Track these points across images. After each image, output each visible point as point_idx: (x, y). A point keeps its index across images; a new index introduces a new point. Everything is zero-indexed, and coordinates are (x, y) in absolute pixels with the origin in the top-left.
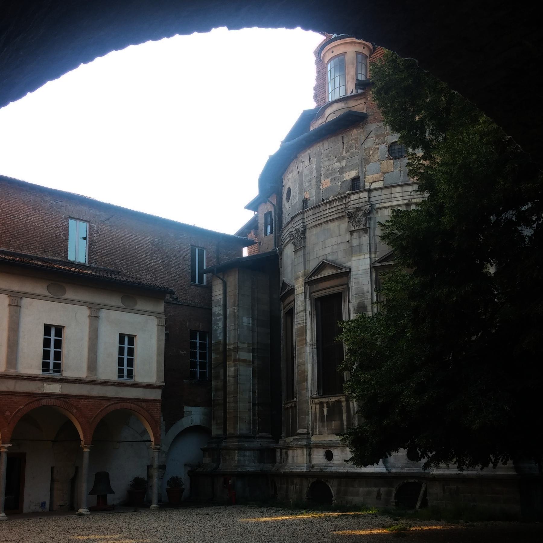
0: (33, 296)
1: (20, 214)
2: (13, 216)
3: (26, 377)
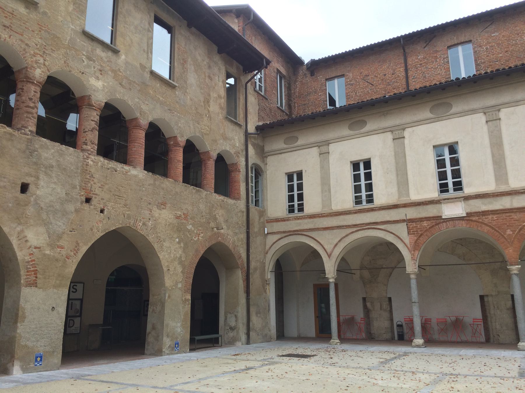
0: (513, 104)
1: (522, 35)
2: (515, 40)
3: (523, 191)
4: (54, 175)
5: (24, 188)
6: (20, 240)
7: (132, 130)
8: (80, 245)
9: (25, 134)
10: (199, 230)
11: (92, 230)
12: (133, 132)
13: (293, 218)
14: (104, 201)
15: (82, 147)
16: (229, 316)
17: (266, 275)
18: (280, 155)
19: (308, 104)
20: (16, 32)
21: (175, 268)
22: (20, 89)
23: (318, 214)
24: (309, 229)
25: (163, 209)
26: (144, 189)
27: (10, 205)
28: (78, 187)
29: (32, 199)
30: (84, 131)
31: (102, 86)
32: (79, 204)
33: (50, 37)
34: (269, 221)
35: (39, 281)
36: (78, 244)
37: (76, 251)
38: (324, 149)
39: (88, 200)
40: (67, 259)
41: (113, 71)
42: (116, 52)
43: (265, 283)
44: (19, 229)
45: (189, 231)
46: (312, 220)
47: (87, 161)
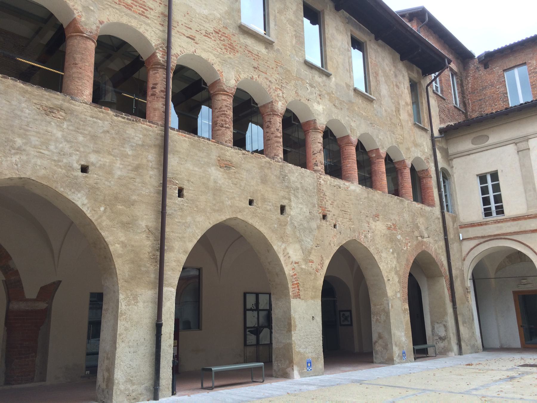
4: (300, 196)
5: (283, 209)
6: (285, 256)
7: (345, 147)
8: (324, 258)
9: (278, 162)
10: (406, 239)
11: (330, 244)
12: (345, 149)
13: (493, 222)
14: (335, 217)
15: (313, 169)
16: (436, 326)
17: (466, 283)
18: (468, 157)
19: (485, 98)
20: (262, 71)
21: (393, 278)
22: (268, 122)
23: (523, 216)
24: (514, 233)
25: (377, 220)
26: (361, 203)
27: (276, 226)
28: (316, 205)
29: (289, 219)
30: (314, 153)
31: (322, 110)
32: (319, 221)
33: (284, 71)
34: (463, 226)
35: (301, 293)
36: (322, 258)
37: (322, 264)
38: (522, 146)
39: (324, 217)
40: (317, 273)
41: (328, 94)
42: (328, 75)
43: (467, 290)
44: (283, 247)
45: (399, 241)
46: (515, 222)
47: (320, 181)
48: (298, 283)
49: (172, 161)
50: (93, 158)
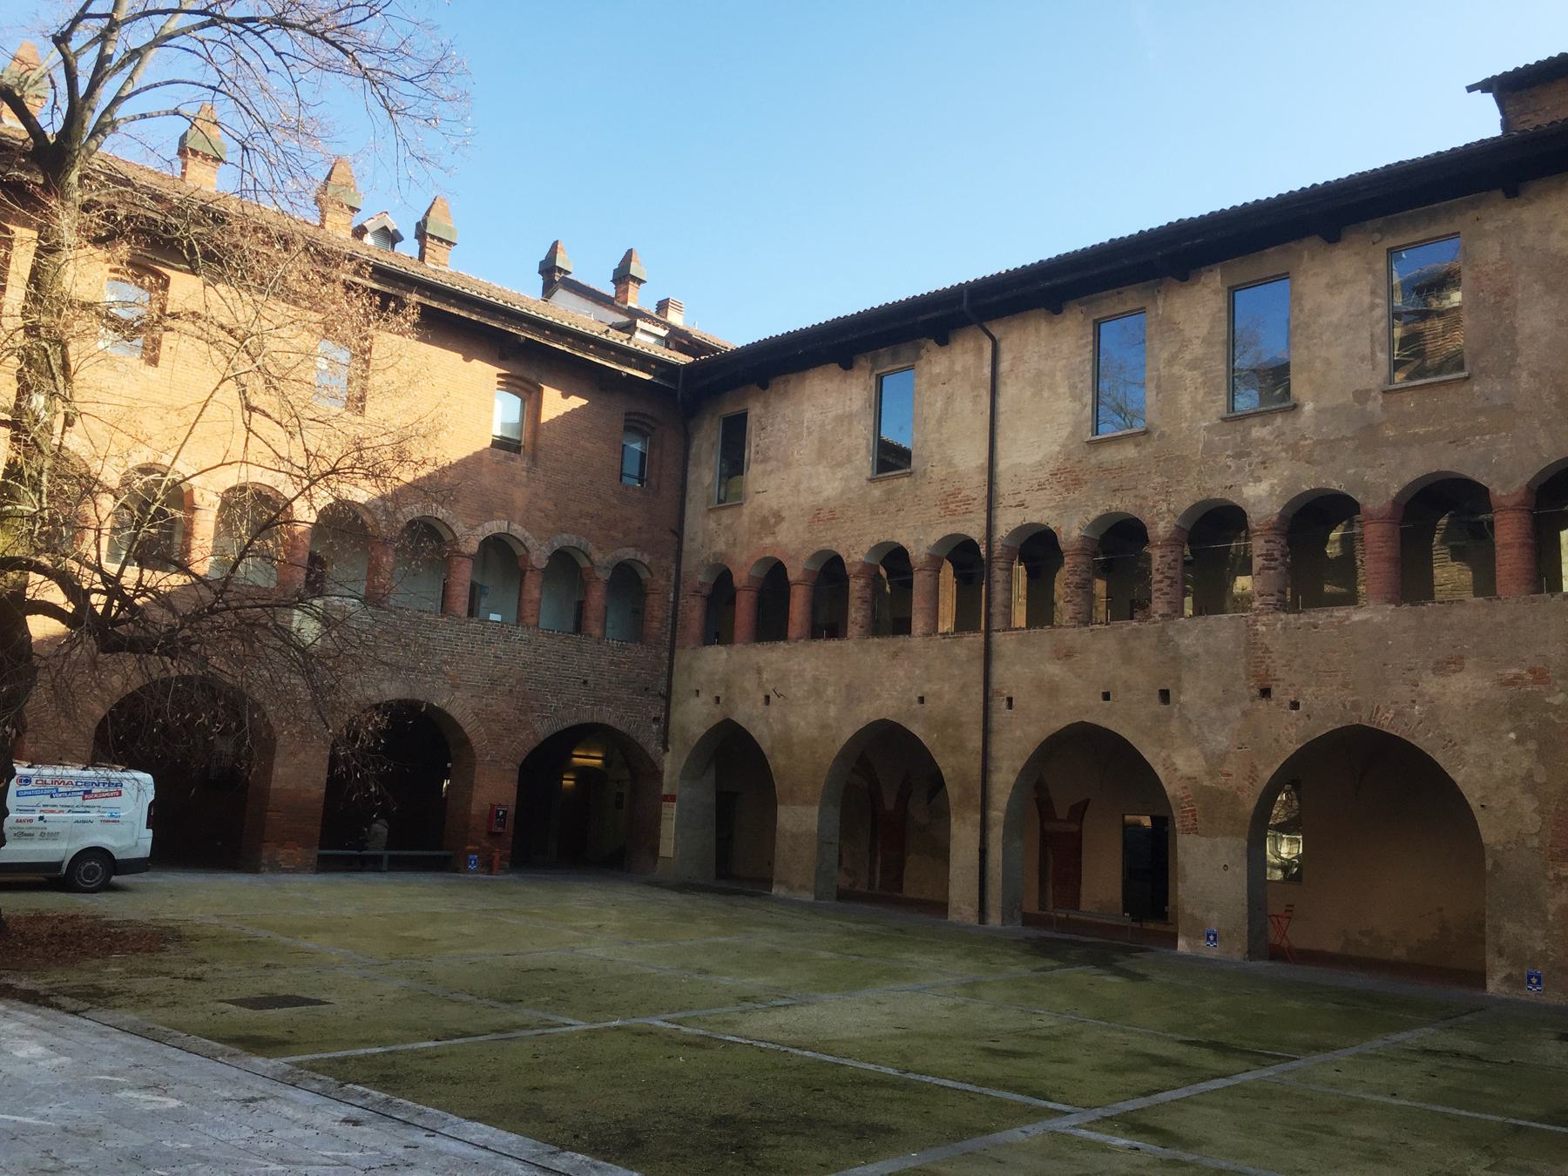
5: (1165, 696)
9: (1155, 622)
11: (1277, 741)
25: (1454, 672)
29: (1176, 710)
32: (1247, 704)
36: (1255, 767)
39: (1266, 693)
44: (1163, 754)
48: (1194, 810)
49: (998, 669)
50: (927, 688)
